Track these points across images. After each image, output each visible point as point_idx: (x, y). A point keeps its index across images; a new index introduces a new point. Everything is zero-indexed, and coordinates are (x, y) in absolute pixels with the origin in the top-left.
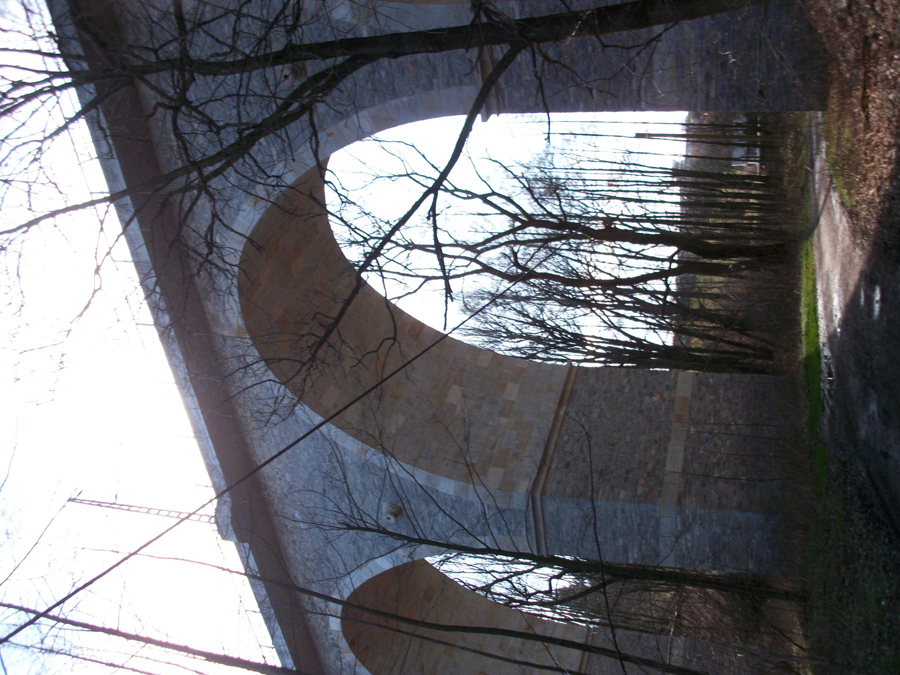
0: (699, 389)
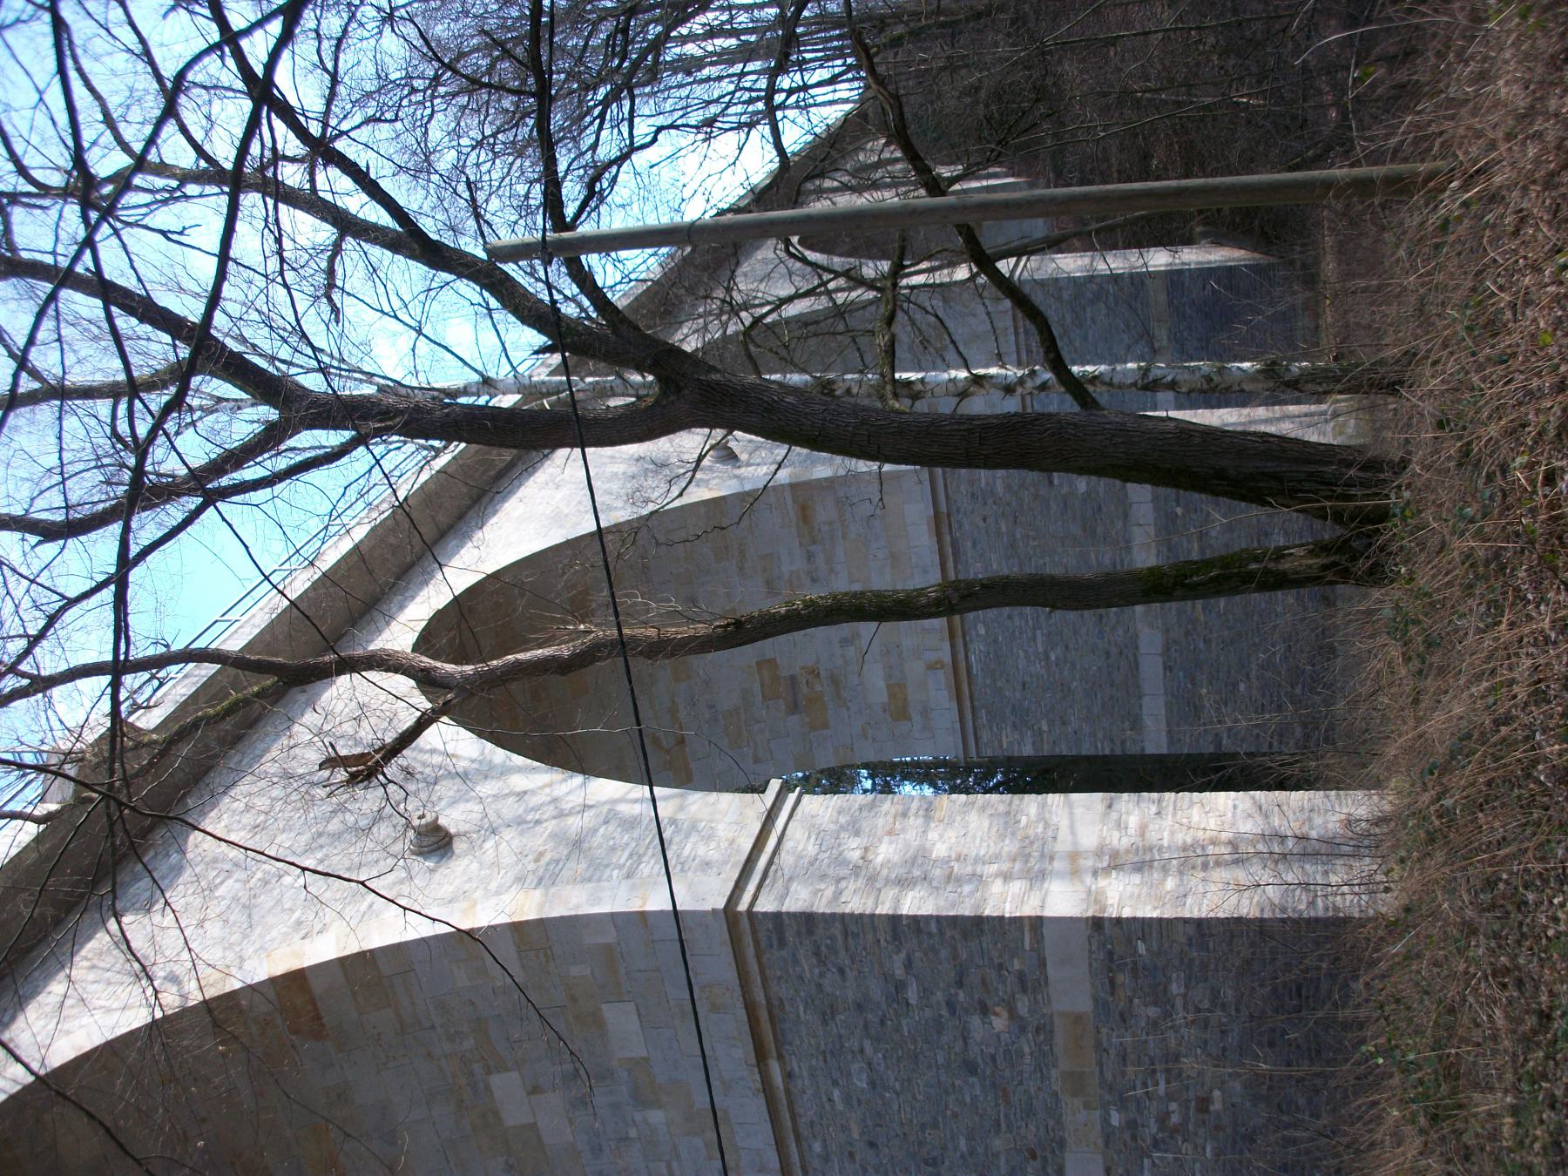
0: (1112, 982)
